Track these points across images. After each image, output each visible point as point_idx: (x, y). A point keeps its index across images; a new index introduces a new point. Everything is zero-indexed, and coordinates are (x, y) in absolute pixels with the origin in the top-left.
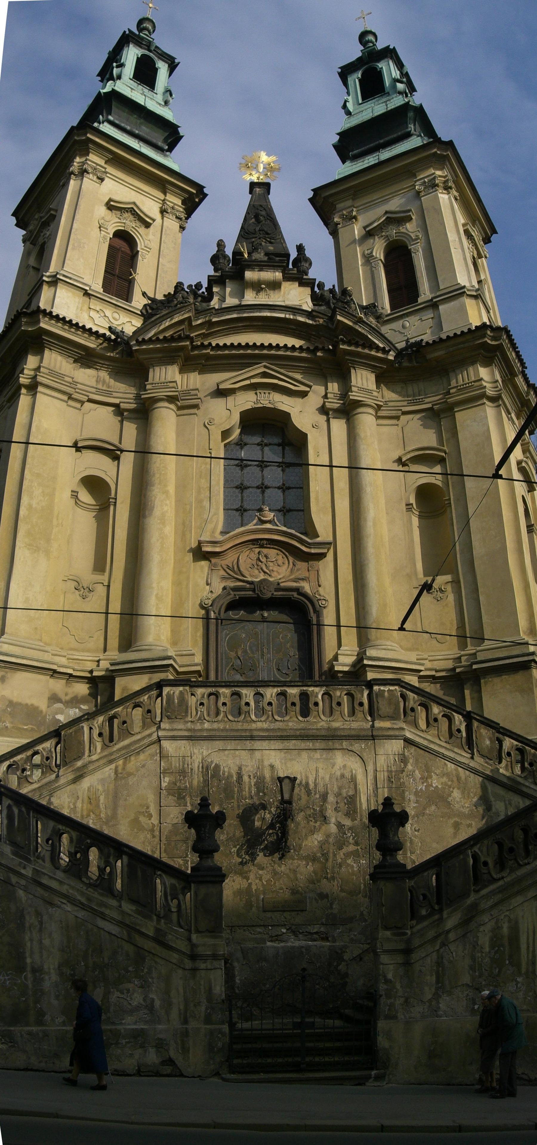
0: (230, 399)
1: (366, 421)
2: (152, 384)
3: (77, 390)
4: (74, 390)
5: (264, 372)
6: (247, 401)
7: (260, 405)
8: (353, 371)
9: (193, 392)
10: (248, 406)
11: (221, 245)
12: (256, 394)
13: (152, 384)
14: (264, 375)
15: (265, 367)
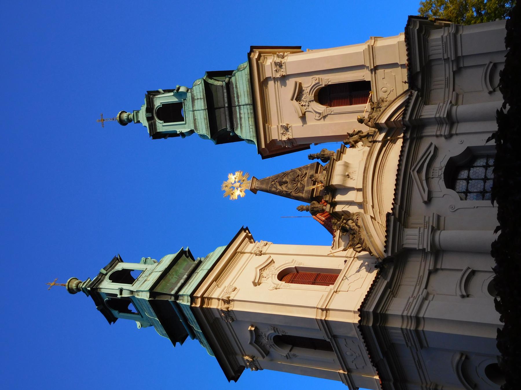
0: (434, 195)
1: (461, 110)
2: (419, 244)
3: (420, 293)
4: (421, 296)
5: (418, 172)
6: (439, 184)
7: (442, 176)
8: (423, 117)
9: (427, 219)
10: (442, 183)
11: (301, 209)
12: (432, 178)
13: (419, 244)
14: (419, 172)
15: (413, 171)
